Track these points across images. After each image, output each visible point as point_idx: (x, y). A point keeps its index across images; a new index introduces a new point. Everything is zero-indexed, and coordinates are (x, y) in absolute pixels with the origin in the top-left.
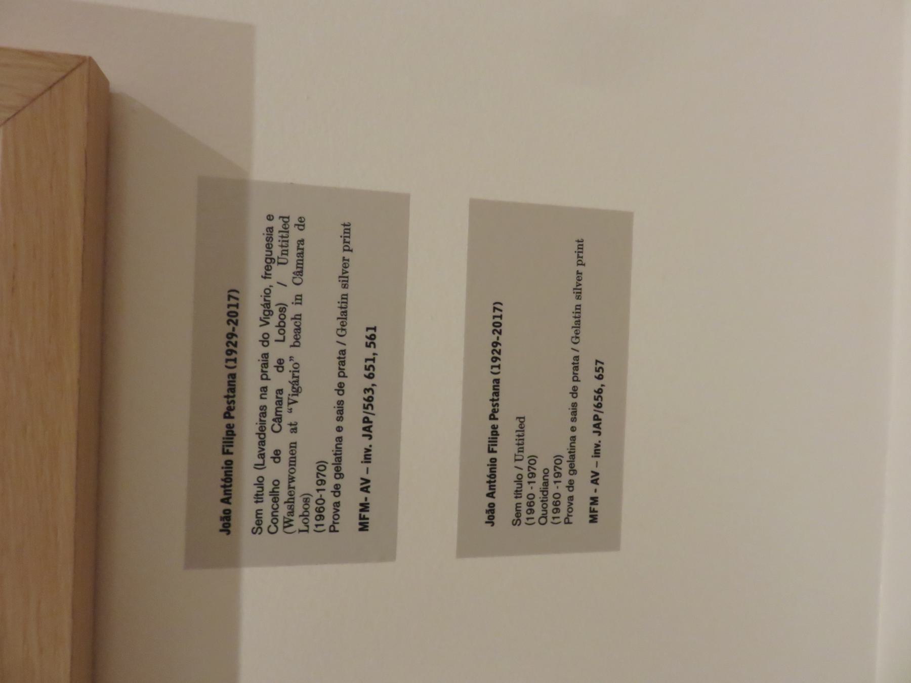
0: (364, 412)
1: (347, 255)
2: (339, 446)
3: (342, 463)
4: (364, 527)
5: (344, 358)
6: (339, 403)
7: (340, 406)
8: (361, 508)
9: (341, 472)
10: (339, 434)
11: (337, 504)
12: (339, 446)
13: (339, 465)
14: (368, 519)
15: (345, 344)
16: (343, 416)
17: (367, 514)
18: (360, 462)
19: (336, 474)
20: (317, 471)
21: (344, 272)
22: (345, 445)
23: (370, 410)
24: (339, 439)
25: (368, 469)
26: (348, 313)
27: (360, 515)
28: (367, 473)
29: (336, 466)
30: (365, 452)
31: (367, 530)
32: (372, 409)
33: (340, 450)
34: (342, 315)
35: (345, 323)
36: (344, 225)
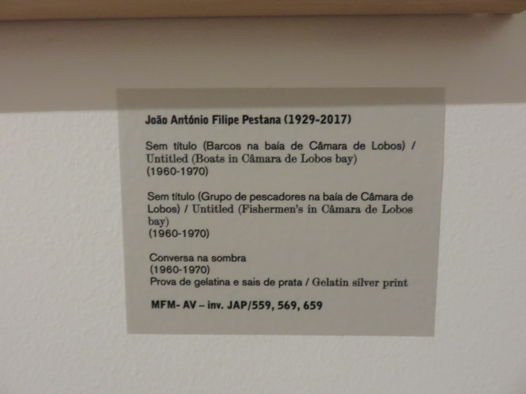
0: (250, 302)
1: (381, 285)
2: (222, 283)
4: (156, 304)
5: (295, 285)
6: (258, 282)
7: (255, 283)
8: (171, 302)
10: (232, 283)
11: (174, 283)
14: (162, 307)
15: (306, 285)
16: (247, 286)
17: (165, 307)
18: (209, 300)
19: (199, 281)
20: (201, 267)
21: (367, 282)
22: (222, 287)
23: (252, 306)
24: (228, 283)
25: (203, 306)
26: (333, 287)
27: (165, 301)
28: (200, 306)
30: (217, 304)
31: (153, 307)
32: (254, 308)
33: (219, 284)
35: (324, 284)
36: (405, 282)
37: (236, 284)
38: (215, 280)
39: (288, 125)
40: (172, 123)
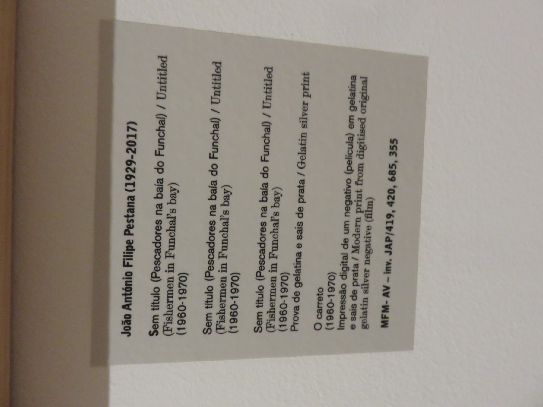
2: (298, 260)
3: (301, 274)
9: (300, 282)
10: (299, 250)
12: (298, 260)
13: (298, 276)
22: (303, 260)
24: (299, 254)
29: (296, 276)
33: (300, 263)
34: (302, 151)
37: (300, 246)
38: (296, 267)
39: (136, 188)
40: (130, 309)
